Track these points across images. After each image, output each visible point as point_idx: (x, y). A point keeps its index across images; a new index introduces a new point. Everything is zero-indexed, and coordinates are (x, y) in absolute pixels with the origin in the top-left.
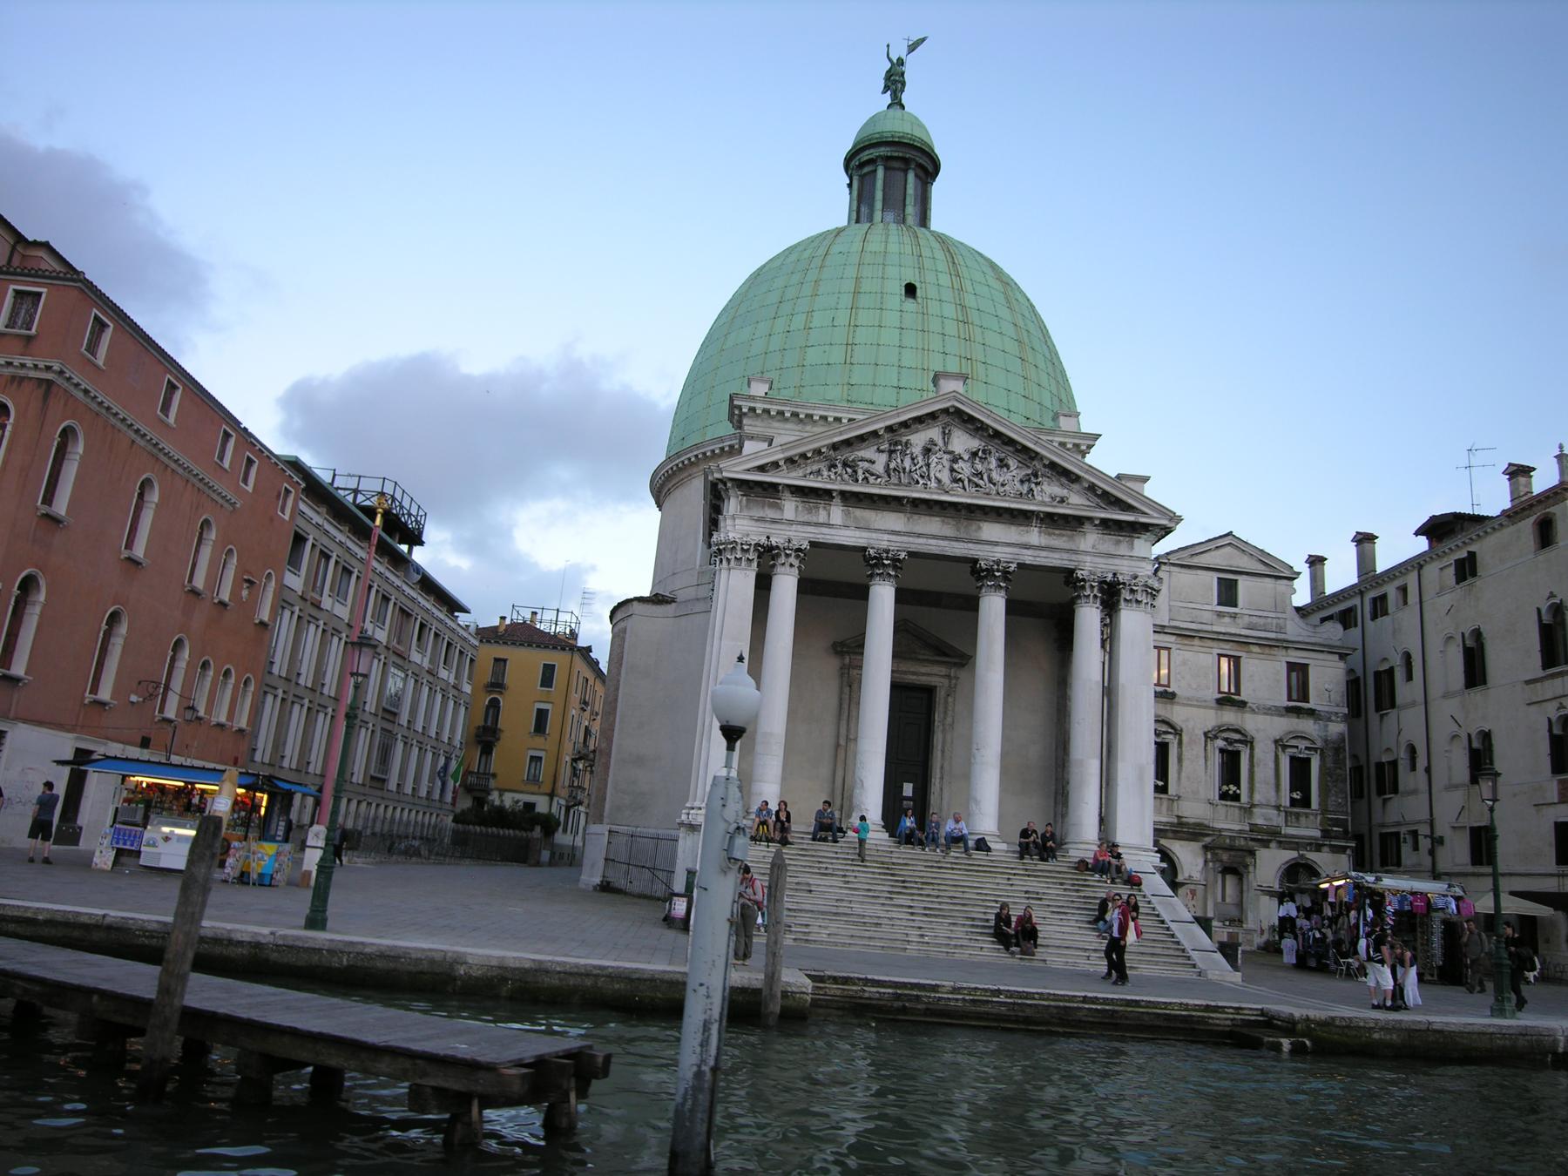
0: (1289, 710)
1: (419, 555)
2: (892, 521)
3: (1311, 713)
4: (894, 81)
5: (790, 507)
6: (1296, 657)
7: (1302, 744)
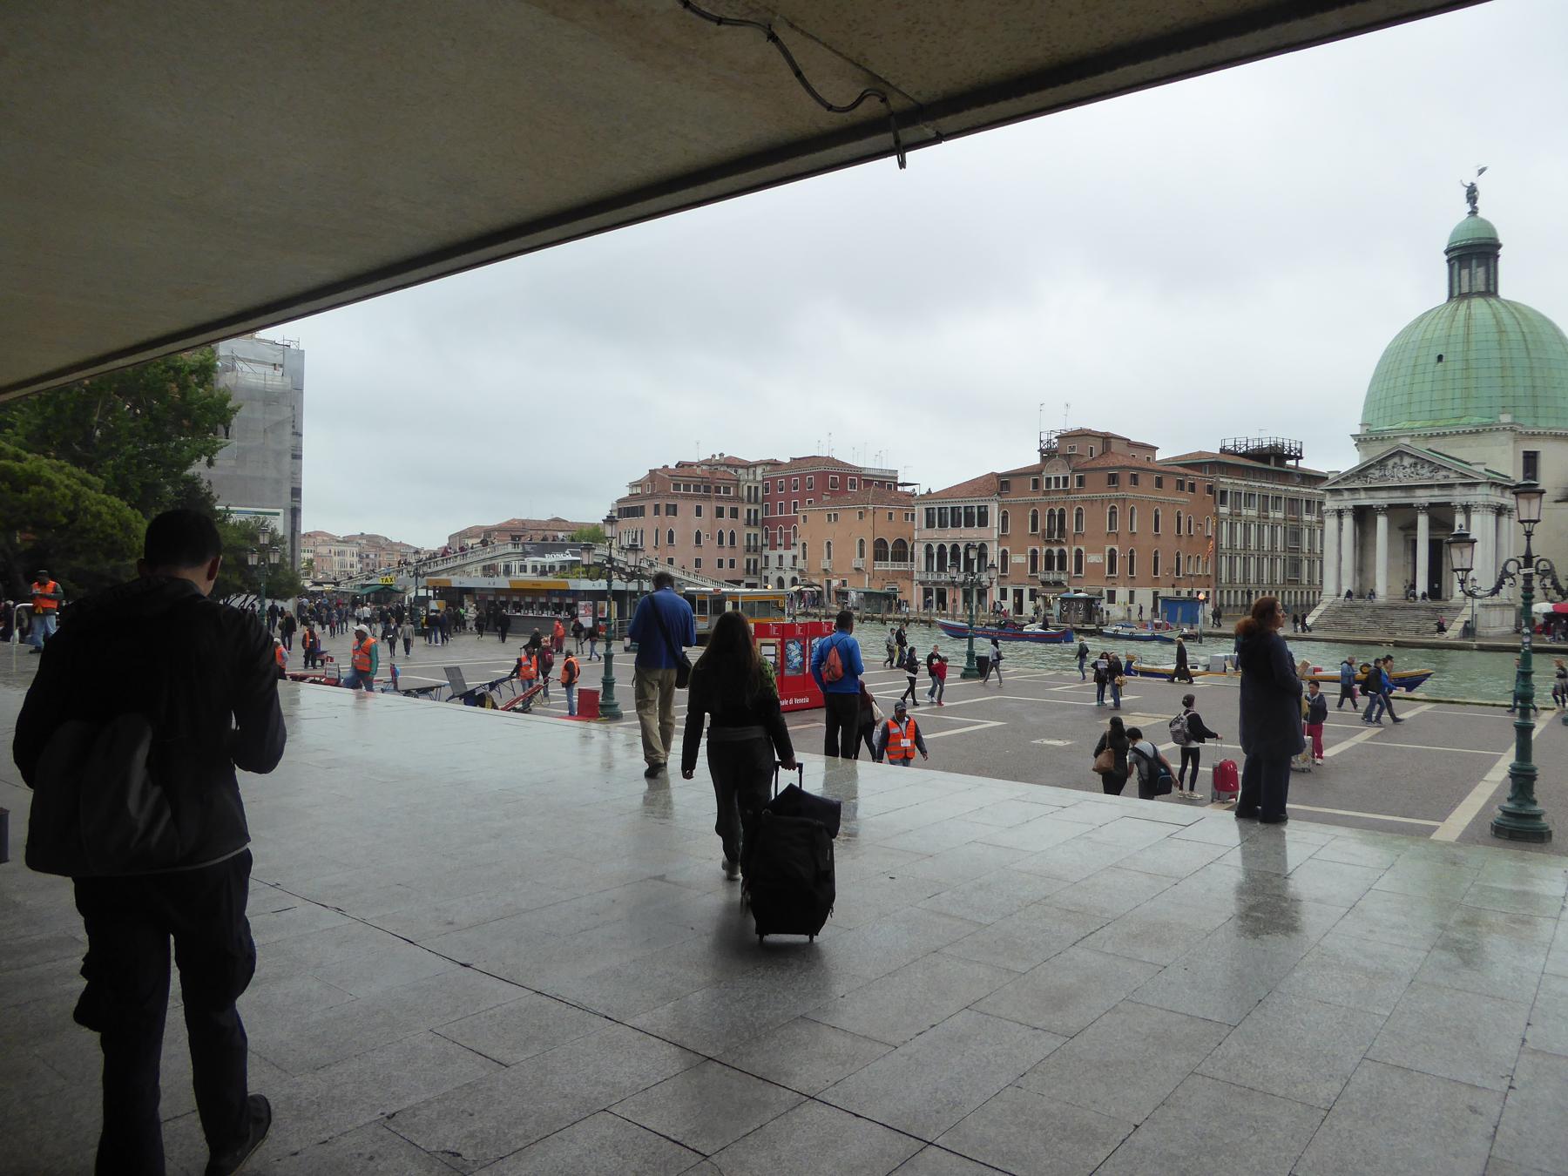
1: (1302, 464)
2: (1384, 494)
4: (1472, 194)
5: (1346, 495)
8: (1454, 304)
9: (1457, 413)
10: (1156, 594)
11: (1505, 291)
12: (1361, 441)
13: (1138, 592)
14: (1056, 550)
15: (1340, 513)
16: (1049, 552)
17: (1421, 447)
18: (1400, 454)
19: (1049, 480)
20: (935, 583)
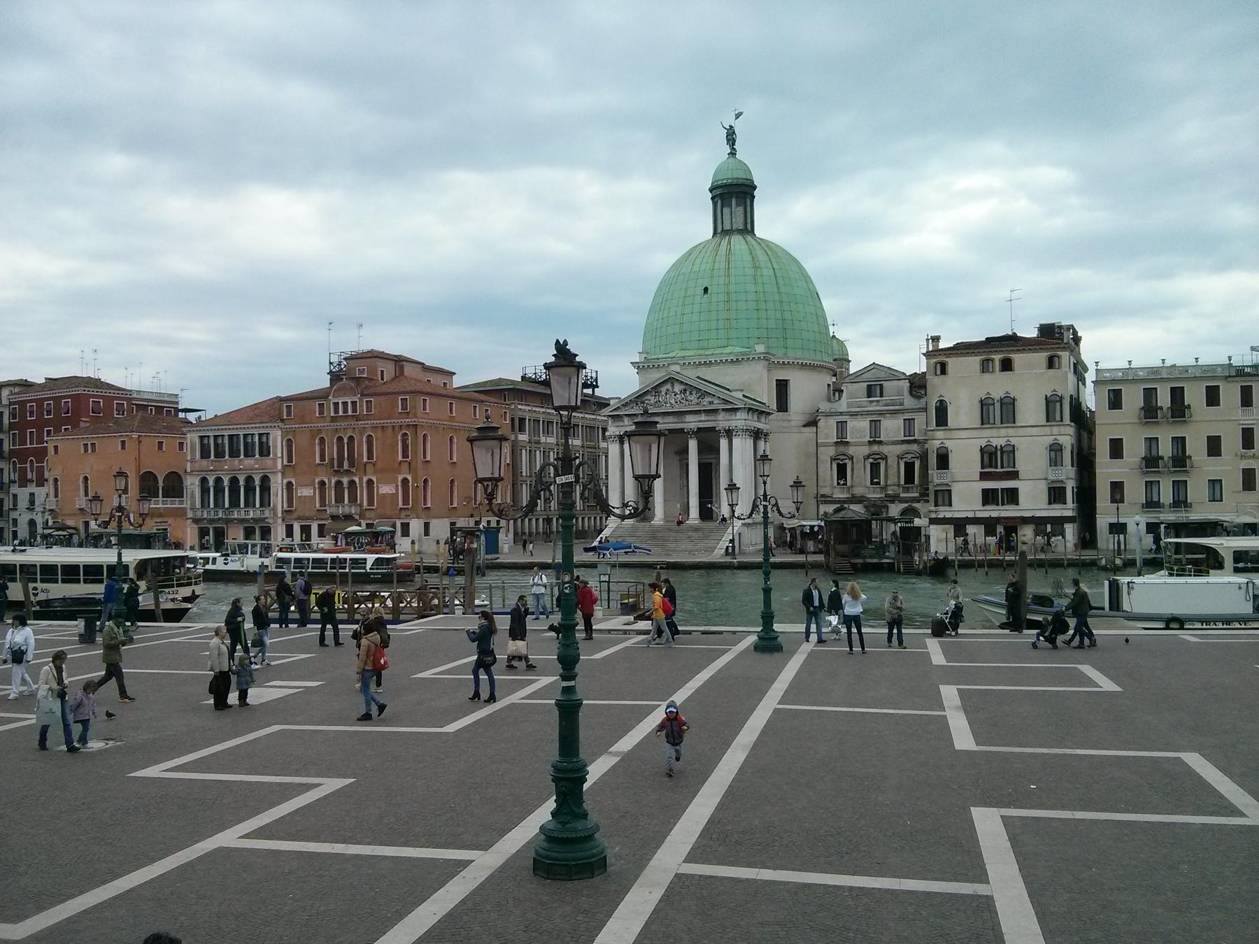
0: (904, 442)
1: (598, 392)
3: (915, 441)
5: (626, 420)
6: (907, 416)
7: (909, 456)
8: (717, 239)
9: (720, 343)
10: (453, 524)
11: (762, 230)
12: (641, 367)
13: (434, 524)
14: (345, 480)
15: (621, 439)
16: (339, 483)
17: (690, 375)
18: (671, 380)
19: (336, 404)
20: (211, 521)
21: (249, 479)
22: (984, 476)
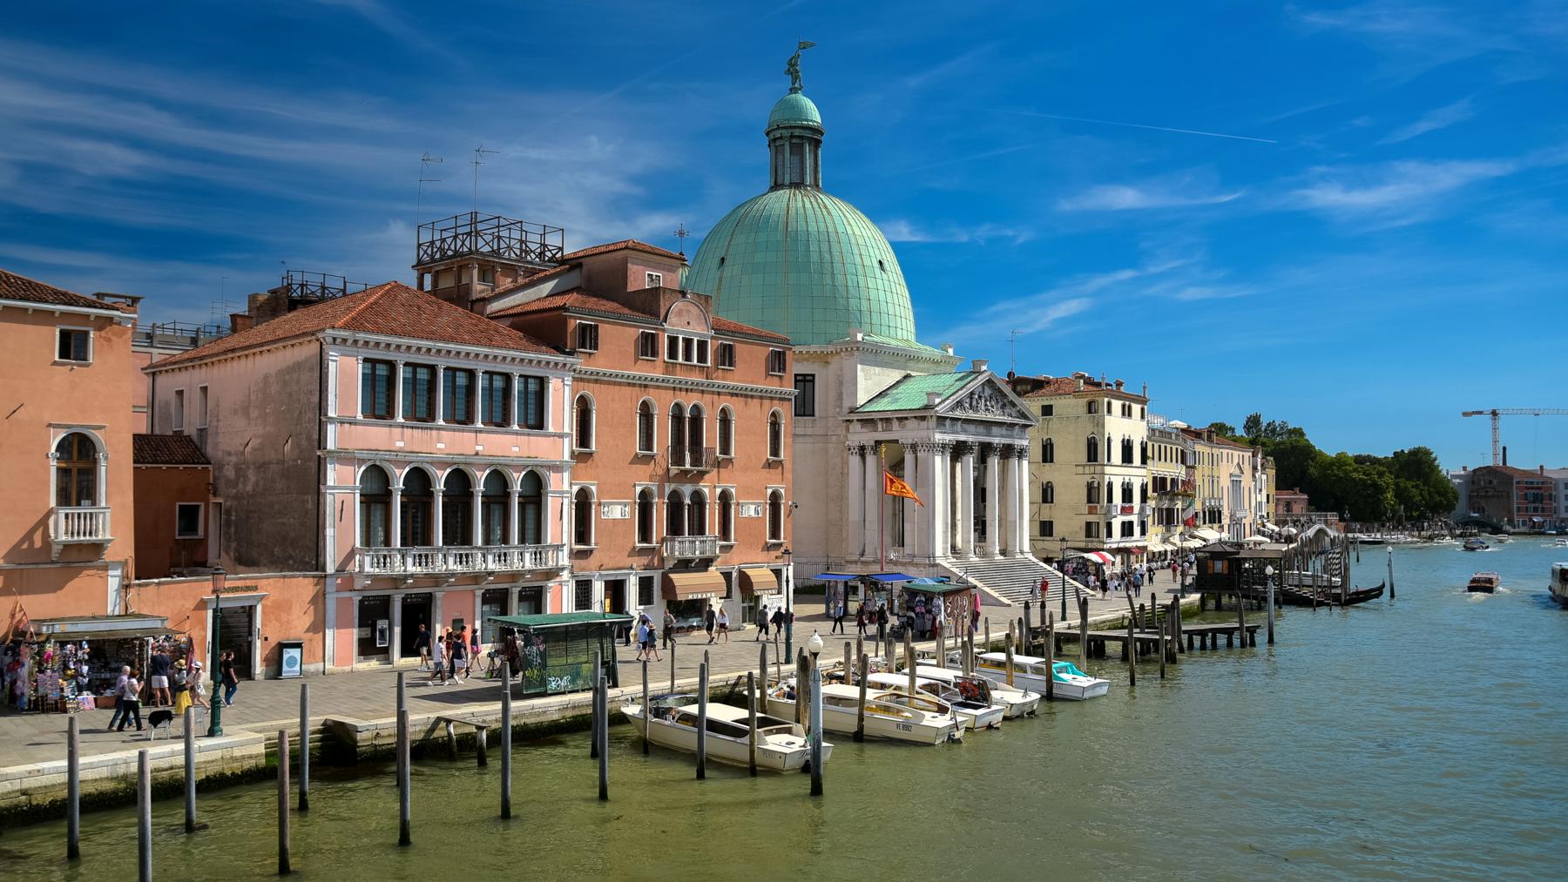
2: (971, 428)
14: (687, 490)
21: (498, 478)
22: (1125, 511)
